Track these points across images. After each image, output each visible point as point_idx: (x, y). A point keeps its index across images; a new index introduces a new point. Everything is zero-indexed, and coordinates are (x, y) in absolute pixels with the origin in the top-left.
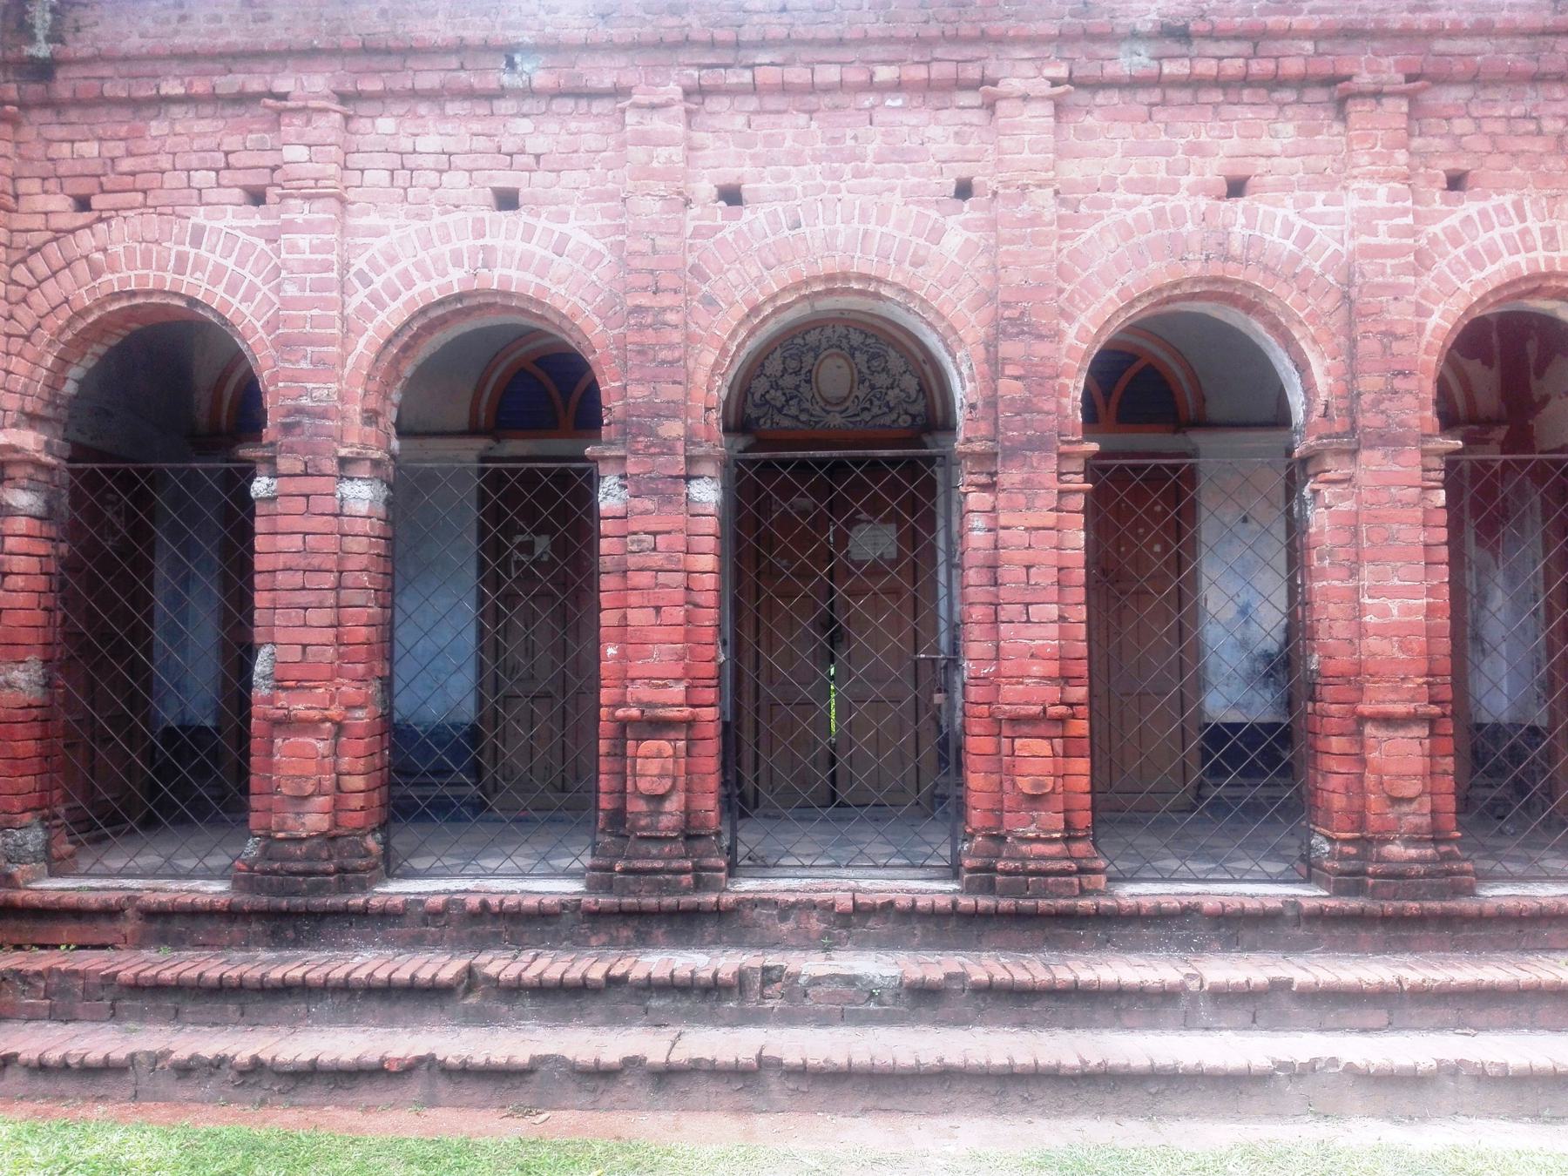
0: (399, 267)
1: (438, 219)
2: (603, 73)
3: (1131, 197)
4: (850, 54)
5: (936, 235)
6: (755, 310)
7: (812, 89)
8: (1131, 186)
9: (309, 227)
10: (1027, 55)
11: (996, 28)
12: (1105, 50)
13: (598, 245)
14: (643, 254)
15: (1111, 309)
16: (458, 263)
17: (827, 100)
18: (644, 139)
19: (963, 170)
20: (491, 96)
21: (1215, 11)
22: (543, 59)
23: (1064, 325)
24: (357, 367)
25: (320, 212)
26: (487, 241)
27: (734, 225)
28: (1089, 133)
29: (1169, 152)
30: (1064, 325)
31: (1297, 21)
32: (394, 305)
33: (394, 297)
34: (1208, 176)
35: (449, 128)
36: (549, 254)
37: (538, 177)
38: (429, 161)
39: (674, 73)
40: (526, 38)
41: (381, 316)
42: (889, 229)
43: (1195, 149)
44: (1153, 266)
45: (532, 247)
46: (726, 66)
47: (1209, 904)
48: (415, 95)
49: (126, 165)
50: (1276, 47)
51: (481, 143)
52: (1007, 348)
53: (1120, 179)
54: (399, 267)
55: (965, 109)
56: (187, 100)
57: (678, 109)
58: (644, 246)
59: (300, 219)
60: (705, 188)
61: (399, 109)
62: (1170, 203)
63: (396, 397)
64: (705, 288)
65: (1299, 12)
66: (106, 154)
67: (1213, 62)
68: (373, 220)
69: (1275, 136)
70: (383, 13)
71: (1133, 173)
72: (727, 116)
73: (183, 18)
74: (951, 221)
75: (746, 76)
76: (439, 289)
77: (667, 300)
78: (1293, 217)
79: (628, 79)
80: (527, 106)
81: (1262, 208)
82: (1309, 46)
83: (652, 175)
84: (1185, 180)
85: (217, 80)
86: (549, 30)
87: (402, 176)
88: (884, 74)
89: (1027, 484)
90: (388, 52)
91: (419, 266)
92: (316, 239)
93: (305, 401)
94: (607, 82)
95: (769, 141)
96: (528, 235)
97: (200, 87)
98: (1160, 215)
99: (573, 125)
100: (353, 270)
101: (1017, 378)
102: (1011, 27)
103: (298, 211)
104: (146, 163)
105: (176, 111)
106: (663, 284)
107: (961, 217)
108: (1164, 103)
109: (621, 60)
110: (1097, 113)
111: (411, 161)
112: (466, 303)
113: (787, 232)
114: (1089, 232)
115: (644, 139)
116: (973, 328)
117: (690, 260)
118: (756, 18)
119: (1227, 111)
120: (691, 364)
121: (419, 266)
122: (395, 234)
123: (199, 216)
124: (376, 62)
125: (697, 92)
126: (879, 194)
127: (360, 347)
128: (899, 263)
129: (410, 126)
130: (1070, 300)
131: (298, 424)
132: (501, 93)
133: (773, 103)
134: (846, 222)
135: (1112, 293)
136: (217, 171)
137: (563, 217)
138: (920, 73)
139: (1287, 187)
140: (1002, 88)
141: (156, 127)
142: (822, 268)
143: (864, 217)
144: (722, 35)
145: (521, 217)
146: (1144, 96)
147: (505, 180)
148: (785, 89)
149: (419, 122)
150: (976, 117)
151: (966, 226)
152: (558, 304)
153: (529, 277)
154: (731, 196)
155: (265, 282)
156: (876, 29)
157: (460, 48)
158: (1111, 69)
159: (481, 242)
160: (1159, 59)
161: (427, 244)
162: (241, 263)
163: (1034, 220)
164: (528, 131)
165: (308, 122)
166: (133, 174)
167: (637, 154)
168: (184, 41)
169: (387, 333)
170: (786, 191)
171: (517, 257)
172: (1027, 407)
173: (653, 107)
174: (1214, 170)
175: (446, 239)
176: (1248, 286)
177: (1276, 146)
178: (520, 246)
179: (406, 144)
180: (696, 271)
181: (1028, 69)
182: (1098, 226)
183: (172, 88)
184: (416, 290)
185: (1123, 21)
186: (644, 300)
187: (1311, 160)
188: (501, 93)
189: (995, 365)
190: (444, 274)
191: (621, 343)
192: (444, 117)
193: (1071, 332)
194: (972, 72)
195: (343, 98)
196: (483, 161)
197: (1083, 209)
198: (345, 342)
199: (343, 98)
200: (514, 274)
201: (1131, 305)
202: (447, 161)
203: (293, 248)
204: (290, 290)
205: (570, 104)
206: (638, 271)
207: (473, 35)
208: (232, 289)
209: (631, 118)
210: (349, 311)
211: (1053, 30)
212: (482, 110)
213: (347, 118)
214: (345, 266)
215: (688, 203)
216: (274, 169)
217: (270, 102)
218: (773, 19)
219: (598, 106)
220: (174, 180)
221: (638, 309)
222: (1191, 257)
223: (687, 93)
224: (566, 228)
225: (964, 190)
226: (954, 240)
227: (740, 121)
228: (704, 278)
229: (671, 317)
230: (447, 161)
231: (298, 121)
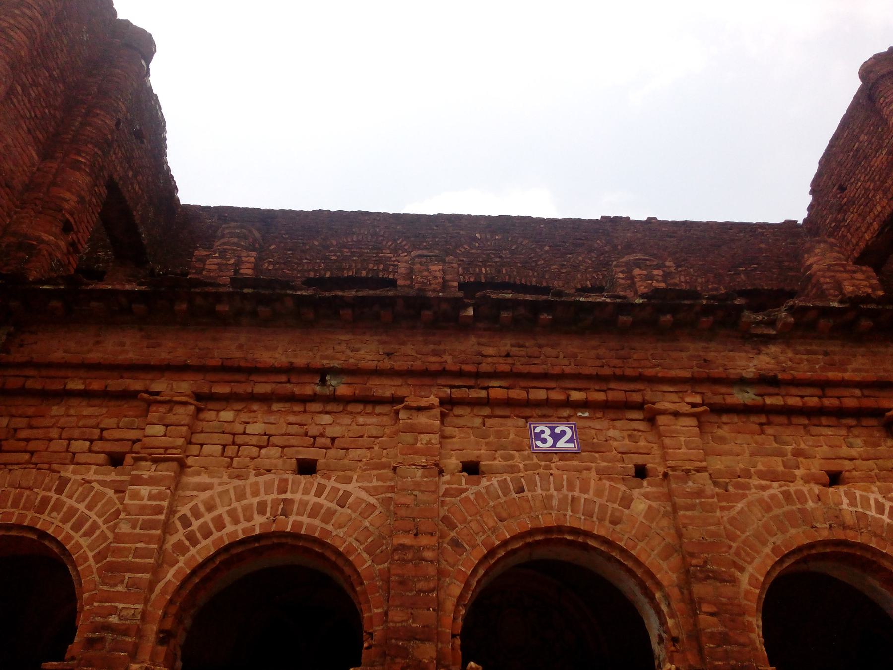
0: (216, 513)
1: (252, 479)
2: (385, 388)
3: (763, 483)
4: (552, 384)
5: (626, 502)
6: (492, 552)
7: (528, 404)
8: (761, 475)
9: (151, 482)
10: (671, 389)
12: (723, 390)
13: (372, 500)
14: (407, 506)
15: (770, 563)
16: (262, 512)
17: (537, 412)
18: (412, 429)
19: (640, 460)
21: (792, 368)
22: (345, 379)
23: (738, 574)
24: (163, 592)
25: (165, 471)
26: (288, 495)
27: (474, 489)
28: (723, 440)
29: (782, 454)
30: (738, 574)
31: (847, 376)
32: (204, 543)
33: (207, 536)
34: (813, 471)
35: (272, 419)
36: (334, 506)
37: (332, 452)
38: (254, 440)
39: (434, 390)
40: (336, 364)
41: (193, 551)
42: (590, 495)
43: (798, 453)
44: (793, 531)
45: (322, 500)
46: (469, 387)
48: (253, 398)
49: (23, 434)
51: (294, 429)
52: (699, 589)
53: (753, 470)
54: (216, 513)
55: (635, 421)
56: (86, 394)
57: (437, 412)
58: (408, 500)
59: (146, 475)
60: (453, 462)
62: (792, 488)
63: (188, 622)
64: (453, 534)
65: (845, 371)
66: (12, 426)
67: (798, 398)
68: (204, 479)
69: (851, 446)
70: (240, 347)
71: (760, 467)
72: (470, 418)
73: (98, 343)
74: (636, 492)
75: (483, 394)
76: (244, 531)
77: (424, 541)
78: (881, 500)
79: (402, 391)
81: (858, 493)
82: (857, 392)
83: (416, 452)
84: (798, 473)
85: (110, 382)
86: (351, 361)
87: (231, 450)
88: (576, 396)
90: (238, 370)
91: (232, 514)
92: (155, 490)
94: (388, 393)
95: (499, 434)
96: (319, 494)
97: (96, 385)
98: (787, 495)
99: (361, 420)
100: (178, 515)
101: (712, 614)
102: (660, 372)
103: (147, 470)
104: (40, 433)
105: (74, 402)
106: (423, 528)
107: (643, 491)
108: (769, 423)
109: (399, 381)
110: (726, 427)
111: (239, 439)
112: (264, 543)
113: (514, 495)
114: (740, 506)
115: (412, 429)
116: (667, 573)
117: (443, 511)
118: (490, 360)
119: (815, 430)
120: (442, 595)
121: (232, 514)
122: (220, 489)
123: (68, 472)
124: (227, 377)
125: (448, 403)
126: (580, 472)
127: (169, 576)
128: (601, 520)
129: (244, 417)
130: (737, 554)
131: (102, 640)
132: (314, 398)
133: (499, 412)
134: (558, 489)
135: (768, 550)
136: (92, 441)
137: (348, 481)
138: (601, 396)
139: (870, 480)
140: (658, 406)
141: (55, 410)
142: (545, 521)
143: (571, 487)
145: (318, 479)
146: (754, 419)
147: (307, 453)
148: (508, 403)
149: (252, 415)
150: (642, 426)
151: (647, 496)
152: (337, 543)
153: (317, 522)
154: (472, 468)
155: (105, 522)
157: (290, 370)
158: (730, 400)
159: (283, 496)
160: (761, 395)
161: (241, 496)
162: (90, 507)
163: (700, 493)
164: (325, 422)
165: (170, 411)
166: (28, 440)
167: (408, 437)
168: (95, 356)
169: (194, 565)
170: (512, 466)
171: (309, 508)
172: (724, 639)
173: (419, 409)
174: (816, 467)
175: (256, 493)
176: (865, 547)
177: (853, 452)
178: (312, 499)
179: (239, 428)
180: (445, 519)
181: (674, 397)
182: (745, 501)
183: (76, 385)
184: (225, 531)
185: (732, 371)
186: (407, 541)
187: (880, 462)
188: (314, 398)
189: (693, 604)
190: (249, 519)
191: (386, 577)
192: (271, 412)
193: (744, 579)
194: (637, 397)
196: (293, 441)
197: (731, 489)
198: (156, 571)
200: (305, 519)
201: (781, 561)
202: (267, 440)
203: (135, 496)
204: (124, 528)
205: (359, 408)
206: (403, 518)
208: (77, 527)
209: (402, 415)
210: (168, 546)
211: (687, 374)
212: (298, 408)
213: (199, 410)
214: (172, 511)
215: (441, 472)
216: (135, 442)
217: (146, 395)
218: (501, 360)
219: (379, 409)
220: (58, 445)
221: (403, 547)
222: (818, 525)
223: (443, 402)
224: (349, 488)
225: (641, 472)
226: (640, 506)
227: (478, 422)
228: (453, 526)
229: (428, 555)
230: (267, 440)
231: (162, 409)
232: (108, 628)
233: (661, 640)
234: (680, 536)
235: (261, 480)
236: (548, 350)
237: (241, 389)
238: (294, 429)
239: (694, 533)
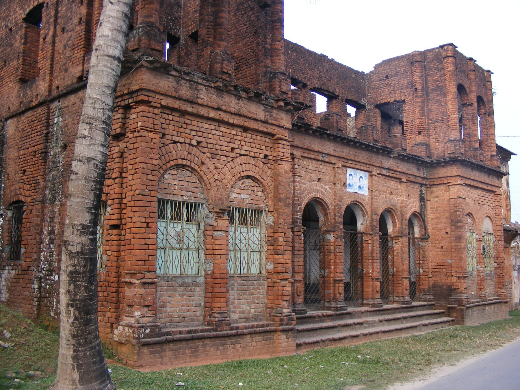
9: (299, 182)
11: (374, 164)
12: (382, 170)
18: (338, 173)
20: (318, 160)
40: (326, 152)
47: (395, 307)
50: (396, 173)
51: (316, 169)
61: (307, 160)
80: (323, 163)
82: (399, 174)
88: (362, 168)
89: (377, 239)
93: (298, 217)
109: (335, 158)
111: (309, 171)
122: (307, 185)
137: (326, 185)
144: (348, 157)
156: (363, 161)
163: (376, 196)
192: (312, 163)
194: (370, 170)
195: (302, 156)
199: (302, 156)
203: (296, 186)
207: (320, 150)
209: (336, 169)
219: (331, 165)
232: (297, 218)
233: (362, 224)
234: (372, 205)
235: (313, 183)
236: (360, 154)
237: (309, 156)
238: (316, 169)
239: (375, 205)
